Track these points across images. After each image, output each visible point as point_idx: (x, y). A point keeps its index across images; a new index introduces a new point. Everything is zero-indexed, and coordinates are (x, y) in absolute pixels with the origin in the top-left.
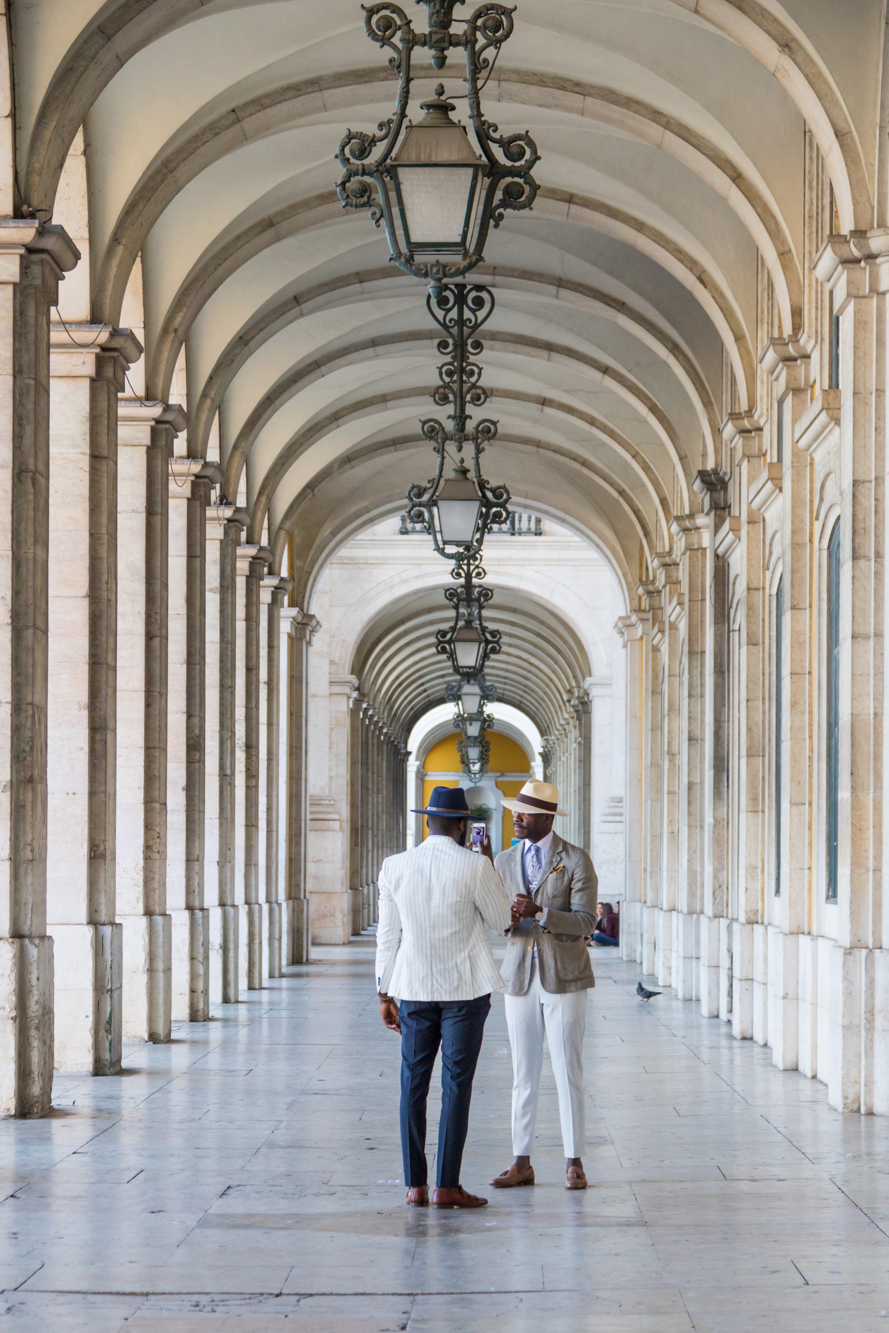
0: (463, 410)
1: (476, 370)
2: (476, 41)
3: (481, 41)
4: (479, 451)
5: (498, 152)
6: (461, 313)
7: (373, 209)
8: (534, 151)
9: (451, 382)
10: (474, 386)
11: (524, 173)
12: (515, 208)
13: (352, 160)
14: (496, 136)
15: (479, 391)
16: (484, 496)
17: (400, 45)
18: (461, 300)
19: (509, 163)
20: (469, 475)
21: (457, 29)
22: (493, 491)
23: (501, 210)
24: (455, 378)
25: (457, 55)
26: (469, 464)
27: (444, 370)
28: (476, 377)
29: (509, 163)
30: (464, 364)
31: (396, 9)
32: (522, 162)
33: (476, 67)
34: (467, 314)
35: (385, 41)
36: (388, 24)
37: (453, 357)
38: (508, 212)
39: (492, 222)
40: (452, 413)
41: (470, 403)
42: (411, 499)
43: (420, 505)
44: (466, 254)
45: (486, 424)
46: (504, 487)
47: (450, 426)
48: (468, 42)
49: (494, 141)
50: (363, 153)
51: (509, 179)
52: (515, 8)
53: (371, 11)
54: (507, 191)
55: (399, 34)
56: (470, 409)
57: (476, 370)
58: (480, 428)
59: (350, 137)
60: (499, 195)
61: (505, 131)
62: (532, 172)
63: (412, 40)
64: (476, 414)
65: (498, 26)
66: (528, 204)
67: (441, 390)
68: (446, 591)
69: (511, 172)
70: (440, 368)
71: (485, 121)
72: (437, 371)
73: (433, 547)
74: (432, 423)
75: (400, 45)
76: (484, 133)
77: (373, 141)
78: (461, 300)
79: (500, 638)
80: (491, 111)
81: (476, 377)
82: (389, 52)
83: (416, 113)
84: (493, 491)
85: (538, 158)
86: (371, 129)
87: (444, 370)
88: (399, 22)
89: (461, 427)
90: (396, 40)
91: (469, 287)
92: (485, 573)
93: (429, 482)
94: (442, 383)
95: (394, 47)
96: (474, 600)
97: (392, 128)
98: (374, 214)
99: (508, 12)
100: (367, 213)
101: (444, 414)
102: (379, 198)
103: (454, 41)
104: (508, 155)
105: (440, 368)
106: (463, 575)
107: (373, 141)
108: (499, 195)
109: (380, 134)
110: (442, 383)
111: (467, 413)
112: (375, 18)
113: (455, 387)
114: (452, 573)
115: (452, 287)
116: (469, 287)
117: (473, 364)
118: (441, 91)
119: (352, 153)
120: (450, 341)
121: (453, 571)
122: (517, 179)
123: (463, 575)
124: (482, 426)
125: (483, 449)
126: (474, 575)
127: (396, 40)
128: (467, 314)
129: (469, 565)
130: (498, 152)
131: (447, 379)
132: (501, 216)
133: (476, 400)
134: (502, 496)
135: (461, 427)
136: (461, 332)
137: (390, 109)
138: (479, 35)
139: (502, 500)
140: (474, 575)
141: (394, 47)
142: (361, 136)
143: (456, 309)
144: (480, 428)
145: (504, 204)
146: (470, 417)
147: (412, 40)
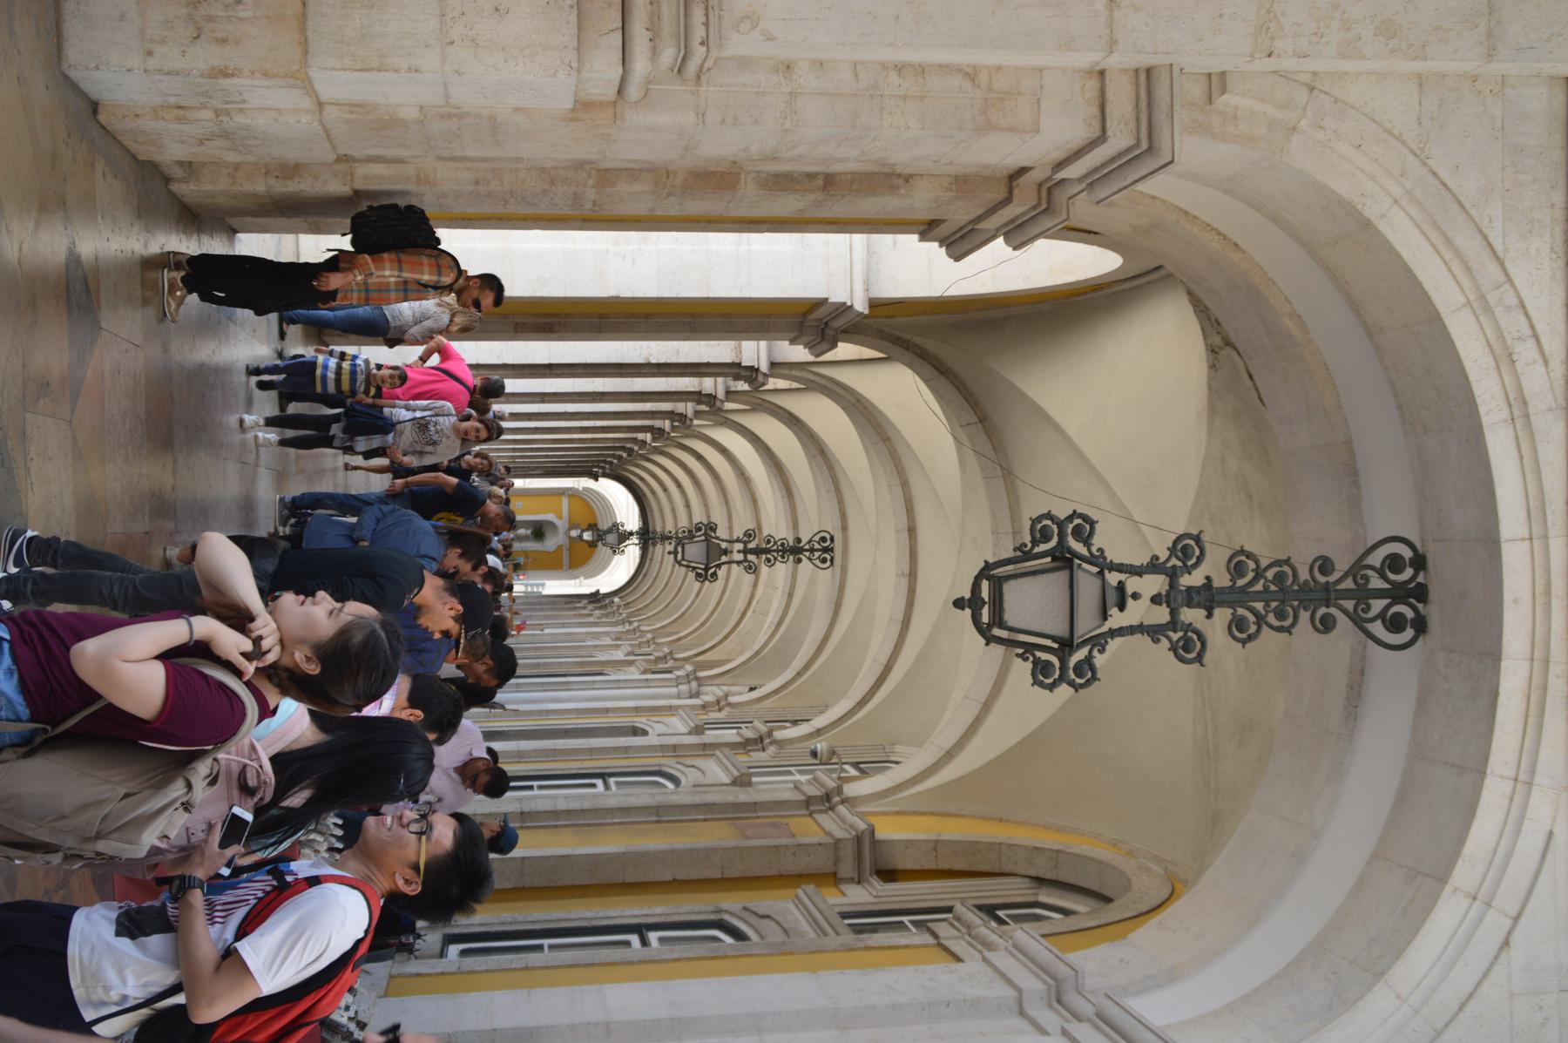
0: (1221, 604)
2: (1175, 631)
3: (1175, 636)
4: (1154, 632)
5: (1081, 654)
8: (1082, 686)
11: (1062, 678)
14: (1095, 653)
16: (1084, 643)
22: (1088, 660)
24: (1273, 588)
25: (1161, 615)
27: (1286, 568)
28: (1276, 623)
31: (1200, 560)
32: (1073, 676)
33: (1155, 632)
35: (1172, 550)
38: (1029, 665)
39: (1020, 651)
40: (1216, 584)
42: (1070, 518)
43: (1062, 535)
44: (990, 626)
45: (1198, 644)
47: (1194, 579)
48: (1174, 624)
49: (1090, 651)
50: (1077, 532)
53: (1197, 539)
54: (1048, 664)
55: (1179, 564)
56: (1222, 615)
59: (1092, 523)
61: (1099, 660)
62: (1064, 685)
63: (1173, 575)
65: (1187, 649)
66: (1036, 682)
69: (1063, 668)
70: (1287, 562)
72: (1283, 557)
76: (1099, 642)
77: (1087, 542)
78: (1398, 593)
79: (1076, 687)
80: (1114, 645)
81: (1276, 623)
84: (1088, 660)
86: (1097, 542)
87: (1286, 568)
89: (1193, 597)
90: (1174, 561)
91: (1420, 606)
92: (1244, 642)
93: (1101, 550)
95: (1168, 560)
99: (1199, 659)
100: (1027, 539)
101: (1212, 569)
102: (1043, 547)
103: (1174, 613)
106: (1241, 583)
107: (1087, 542)
109: (1094, 549)
110: (1264, 563)
111: (1217, 611)
112: (1192, 542)
114: (1242, 552)
115: (1420, 579)
116: (1420, 606)
117: (1296, 618)
120: (1331, 579)
121: (1249, 556)
123: (1241, 583)
126: (1241, 611)
127: (1174, 561)
129: (1264, 595)
130: (1081, 654)
132: (1026, 659)
133: (1238, 624)
134: (1080, 677)
135: (1193, 597)
136: (1347, 594)
137: (1113, 556)
145: (1036, 662)
146: (1209, 616)
147: (1173, 575)
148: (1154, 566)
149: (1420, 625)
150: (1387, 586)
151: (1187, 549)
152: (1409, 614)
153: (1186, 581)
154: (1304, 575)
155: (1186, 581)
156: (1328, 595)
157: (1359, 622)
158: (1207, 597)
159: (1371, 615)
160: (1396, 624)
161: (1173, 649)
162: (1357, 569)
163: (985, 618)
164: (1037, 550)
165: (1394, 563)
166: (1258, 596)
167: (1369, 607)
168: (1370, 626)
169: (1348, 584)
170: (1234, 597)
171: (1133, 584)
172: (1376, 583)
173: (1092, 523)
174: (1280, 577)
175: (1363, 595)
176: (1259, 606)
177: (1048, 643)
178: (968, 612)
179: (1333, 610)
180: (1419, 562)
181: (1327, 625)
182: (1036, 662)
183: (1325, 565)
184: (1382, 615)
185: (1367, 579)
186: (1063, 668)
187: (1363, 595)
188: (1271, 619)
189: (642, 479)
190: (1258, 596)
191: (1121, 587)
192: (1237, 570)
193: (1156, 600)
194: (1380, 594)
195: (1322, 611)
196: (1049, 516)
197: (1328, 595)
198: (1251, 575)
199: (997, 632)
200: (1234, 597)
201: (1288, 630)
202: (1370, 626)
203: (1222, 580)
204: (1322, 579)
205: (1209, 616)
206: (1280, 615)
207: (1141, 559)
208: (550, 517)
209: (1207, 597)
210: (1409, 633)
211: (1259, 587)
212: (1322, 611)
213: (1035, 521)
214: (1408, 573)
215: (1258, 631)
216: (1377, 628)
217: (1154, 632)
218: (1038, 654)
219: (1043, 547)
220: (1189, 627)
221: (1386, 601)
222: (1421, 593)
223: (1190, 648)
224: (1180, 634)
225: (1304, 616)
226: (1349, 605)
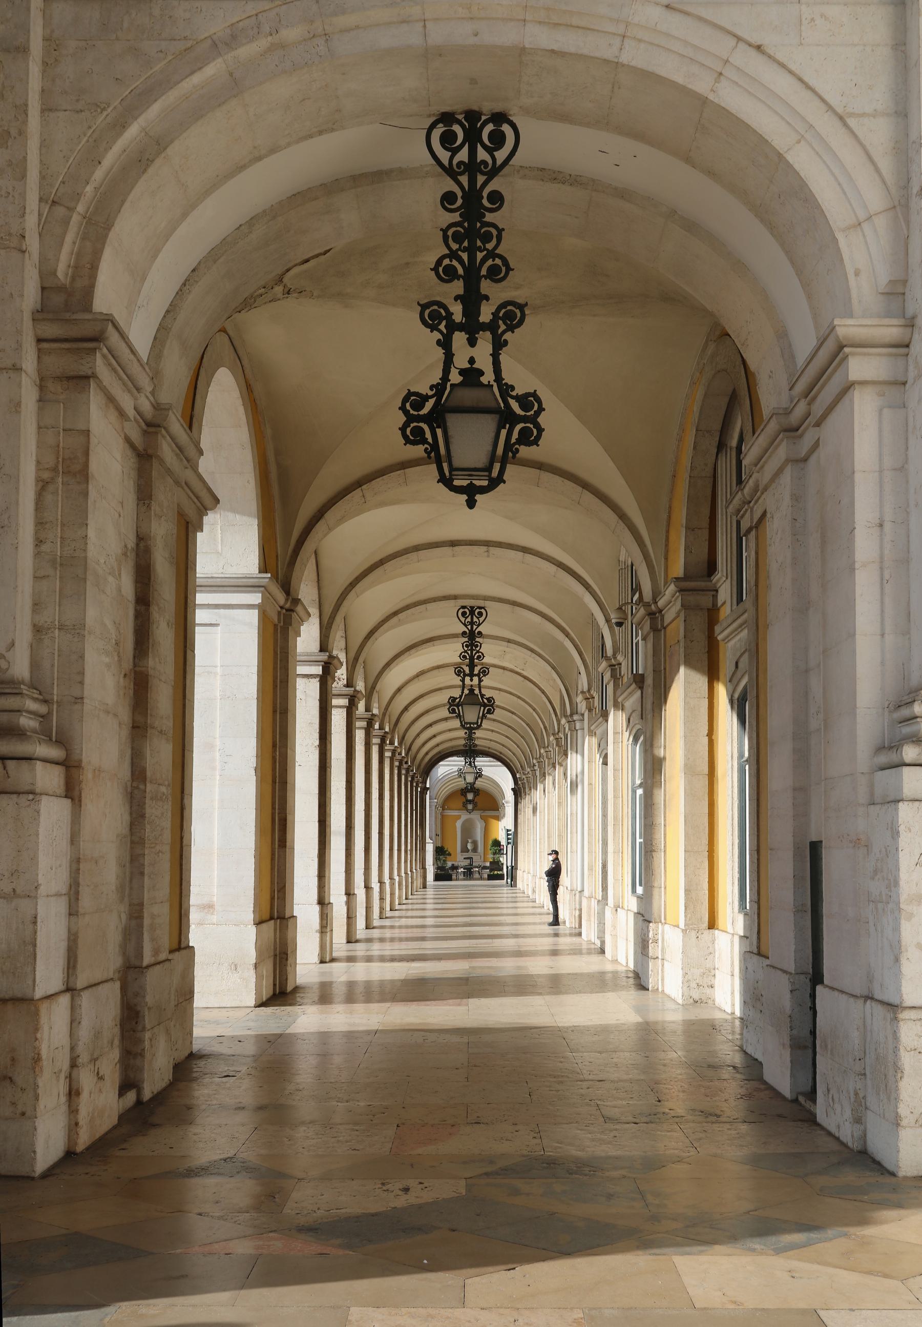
1: (494, 232)
3: (503, 327)
4: (499, 345)
6: (473, 153)
7: (426, 446)
9: (460, 249)
10: (492, 254)
12: (526, 445)
13: (412, 412)
14: (514, 393)
15: (498, 261)
17: (445, 331)
18: (472, 137)
19: (523, 413)
20: (484, 380)
21: (485, 315)
23: (517, 446)
24: (466, 244)
26: (484, 363)
27: (450, 233)
29: (523, 413)
30: (478, 225)
32: (532, 412)
34: (482, 155)
35: (433, 328)
36: (435, 316)
37: (461, 215)
39: (510, 454)
40: (461, 291)
41: (486, 277)
42: (406, 412)
45: (509, 308)
46: (534, 395)
47: (457, 311)
48: (491, 327)
50: (418, 406)
51: (521, 425)
52: (526, 304)
53: (424, 307)
54: (522, 431)
55: (444, 323)
56: (486, 286)
57: (494, 232)
58: (501, 315)
59: (410, 394)
60: (515, 435)
61: (519, 391)
64: (496, 294)
66: (536, 442)
67: (446, 262)
68: (424, 307)
69: (524, 419)
70: (445, 231)
71: (506, 384)
73: (436, 475)
74: (436, 307)
75: (445, 331)
77: (426, 398)
78: (472, 137)
82: (437, 336)
83: (455, 377)
85: (544, 410)
86: (424, 390)
87: (450, 233)
88: (444, 314)
90: (442, 327)
91: (484, 118)
92: (509, 269)
94: (448, 252)
95: (440, 331)
96: (484, 327)
97: (439, 389)
98: (426, 449)
99: (521, 307)
102: (428, 435)
103: (484, 327)
104: (522, 407)
105: (445, 231)
106: (460, 271)
107: (426, 398)
108: (515, 435)
109: (430, 393)
112: (427, 312)
113: (465, 256)
115: (460, 117)
116: (484, 118)
118: (472, 361)
119: (411, 406)
120: (459, 194)
121: (439, 262)
122: (528, 425)
123: (460, 271)
124: (504, 311)
125: (506, 343)
126: (484, 272)
128: (482, 155)
131: (454, 246)
133: (494, 274)
136: (472, 181)
138: (501, 322)
139: (532, 412)
140: (484, 272)
141: (440, 331)
142: (416, 394)
143: (466, 149)
144: (501, 315)
145: (520, 441)
146: (487, 298)
147: (453, 327)
148: (446, 344)
149: (500, 118)
150: (466, 149)
151: (432, 315)
152: (490, 127)
153: (458, 317)
154: (456, 217)
155: (458, 317)
156: (472, 195)
157: (495, 171)
158: (472, 299)
159: (490, 161)
160: (498, 139)
161: (511, 328)
162: (451, 172)
163: (485, 483)
164: (430, 440)
165: (447, 139)
166: (472, 258)
167: (484, 162)
168: (499, 162)
169: (464, 179)
170: (472, 278)
171: (461, 361)
172: (463, 155)
173: (410, 394)
174: (457, 238)
175: (472, 167)
176: (480, 256)
177: (504, 432)
178: (478, 497)
179: (485, 194)
180: (446, 118)
181: (497, 198)
182: (520, 441)
183: (447, 198)
184: (490, 151)
185: (460, 163)
186: (524, 419)
187: (472, 167)
188: (490, 246)
189: (427, 753)
190: (472, 258)
191: (462, 372)
192: (449, 275)
193: (472, 342)
194: (473, 153)
195: (485, 202)
196: (403, 429)
197: (472, 195)
198: (455, 263)
199: (495, 473)
200: (472, 278)
201: (500, 231)
202: (499, 162)
203: (458, 287)
204: (460, 202)
205: (487, 298)
206: (487, 238)
207: (440, 352)
208: (459, 824)
209: (472, 299)
210: (506, 128)
211: (465, 256)
212: (485, 202)
213: (407, 441)
214: (457, 128)
215: (501, 257)
216: (501, 155)
217: (499, 345)
218: (513, 440)
219: (428, 435)
220: (495, 314)
221: (480, 148)
222: (472, 116)
223: (512, 316)
224: (501, 322)
225: (489, 217)
226: (481, 179)
